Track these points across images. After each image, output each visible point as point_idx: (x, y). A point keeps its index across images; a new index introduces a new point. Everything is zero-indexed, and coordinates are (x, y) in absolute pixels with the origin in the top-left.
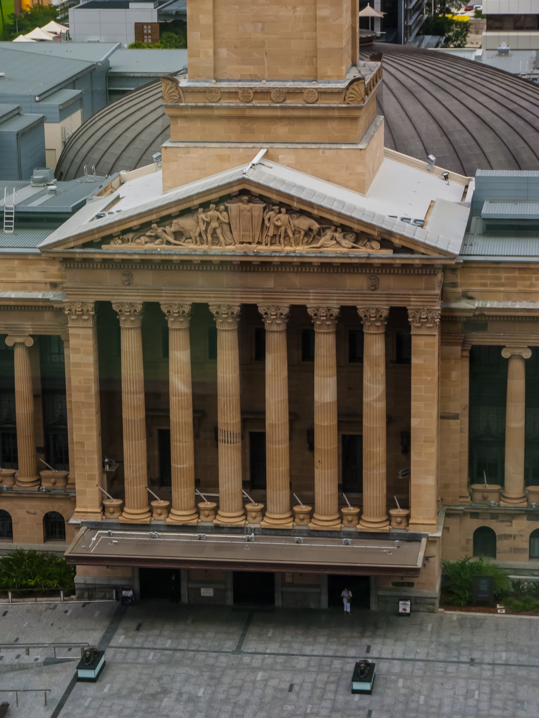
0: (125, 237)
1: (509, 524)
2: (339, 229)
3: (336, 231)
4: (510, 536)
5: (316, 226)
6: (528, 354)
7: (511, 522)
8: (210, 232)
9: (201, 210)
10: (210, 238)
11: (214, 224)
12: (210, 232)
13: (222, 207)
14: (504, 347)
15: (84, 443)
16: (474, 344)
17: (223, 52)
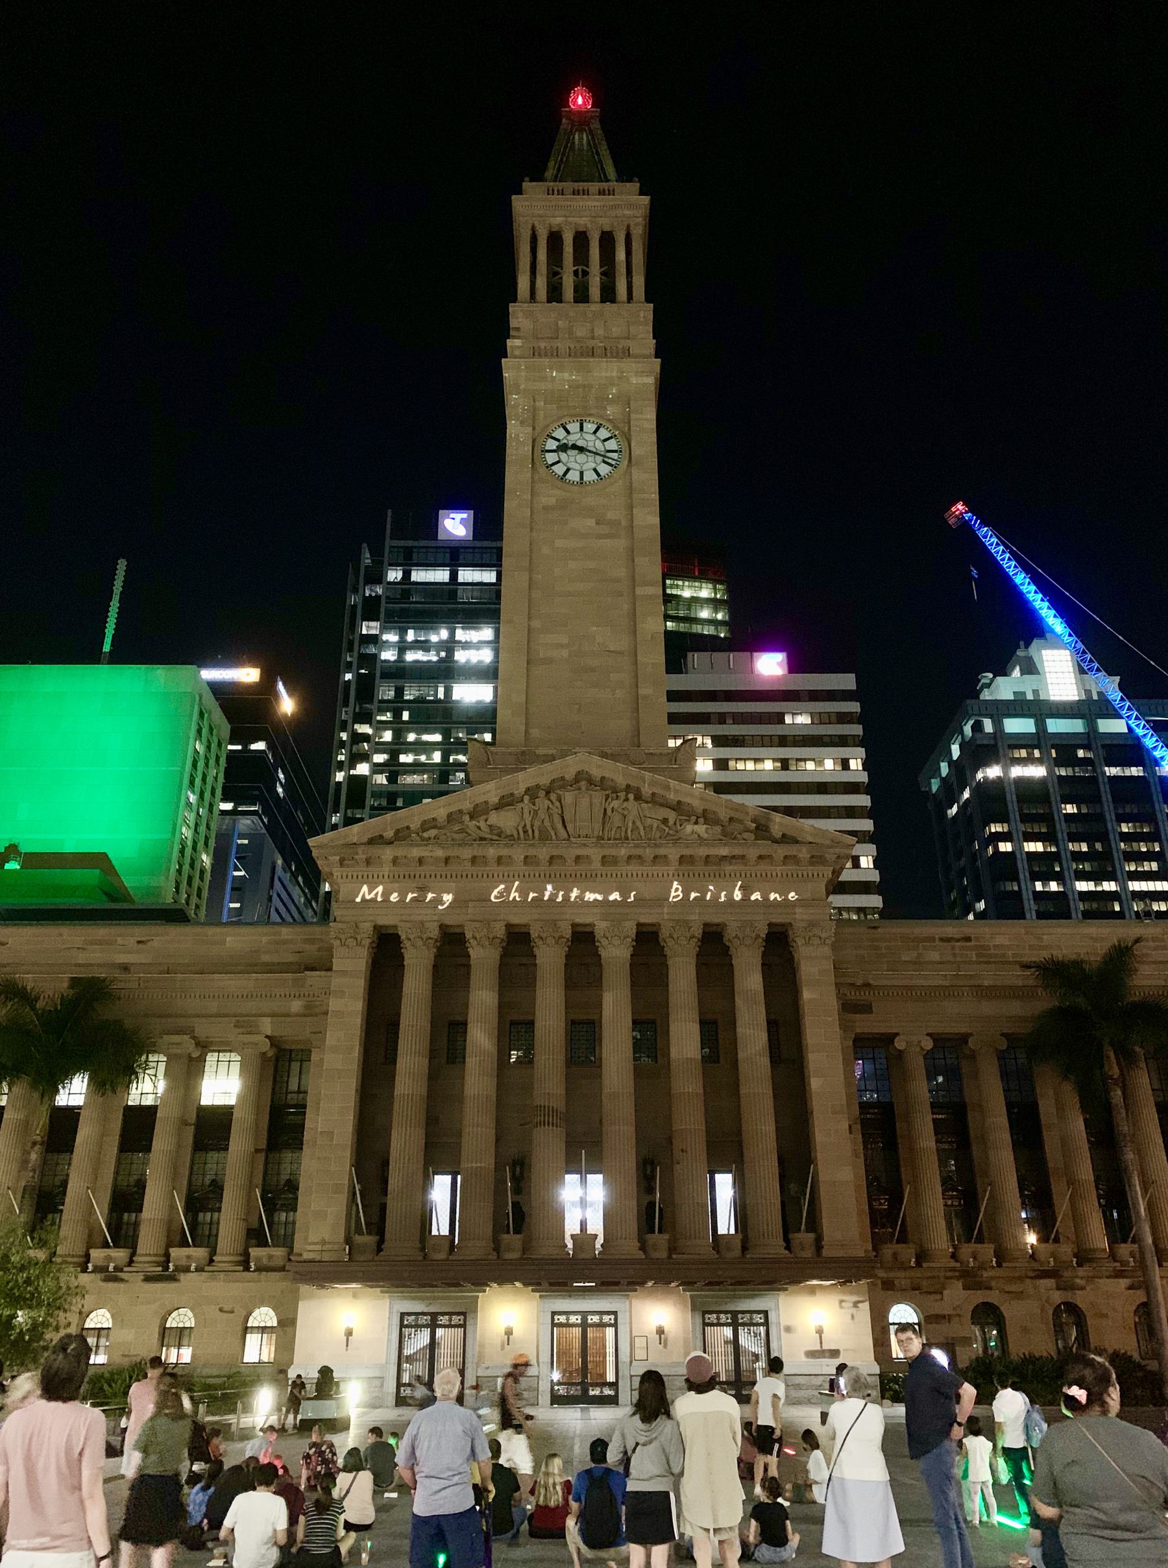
0: (425, 835)
1: (939, 1297)
2: (701, 820)
3: (696, 823)
4: (944, 1317)
5: (672, 816)
6: (928, 1044)
7: (941, 1293)
8: (537, 823)
9: (526, 798)
10: (537, 833)
11: (542, 814)
12: (537, 823)
13: (553, 797)
14: (897, 1034)
15: (332, 1133)
16: (858, 1031)
17: (535, 732)
